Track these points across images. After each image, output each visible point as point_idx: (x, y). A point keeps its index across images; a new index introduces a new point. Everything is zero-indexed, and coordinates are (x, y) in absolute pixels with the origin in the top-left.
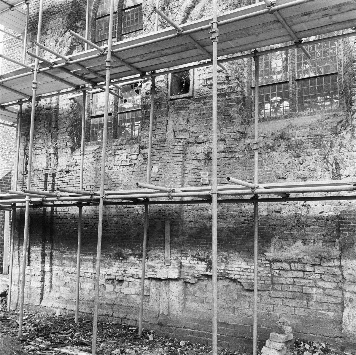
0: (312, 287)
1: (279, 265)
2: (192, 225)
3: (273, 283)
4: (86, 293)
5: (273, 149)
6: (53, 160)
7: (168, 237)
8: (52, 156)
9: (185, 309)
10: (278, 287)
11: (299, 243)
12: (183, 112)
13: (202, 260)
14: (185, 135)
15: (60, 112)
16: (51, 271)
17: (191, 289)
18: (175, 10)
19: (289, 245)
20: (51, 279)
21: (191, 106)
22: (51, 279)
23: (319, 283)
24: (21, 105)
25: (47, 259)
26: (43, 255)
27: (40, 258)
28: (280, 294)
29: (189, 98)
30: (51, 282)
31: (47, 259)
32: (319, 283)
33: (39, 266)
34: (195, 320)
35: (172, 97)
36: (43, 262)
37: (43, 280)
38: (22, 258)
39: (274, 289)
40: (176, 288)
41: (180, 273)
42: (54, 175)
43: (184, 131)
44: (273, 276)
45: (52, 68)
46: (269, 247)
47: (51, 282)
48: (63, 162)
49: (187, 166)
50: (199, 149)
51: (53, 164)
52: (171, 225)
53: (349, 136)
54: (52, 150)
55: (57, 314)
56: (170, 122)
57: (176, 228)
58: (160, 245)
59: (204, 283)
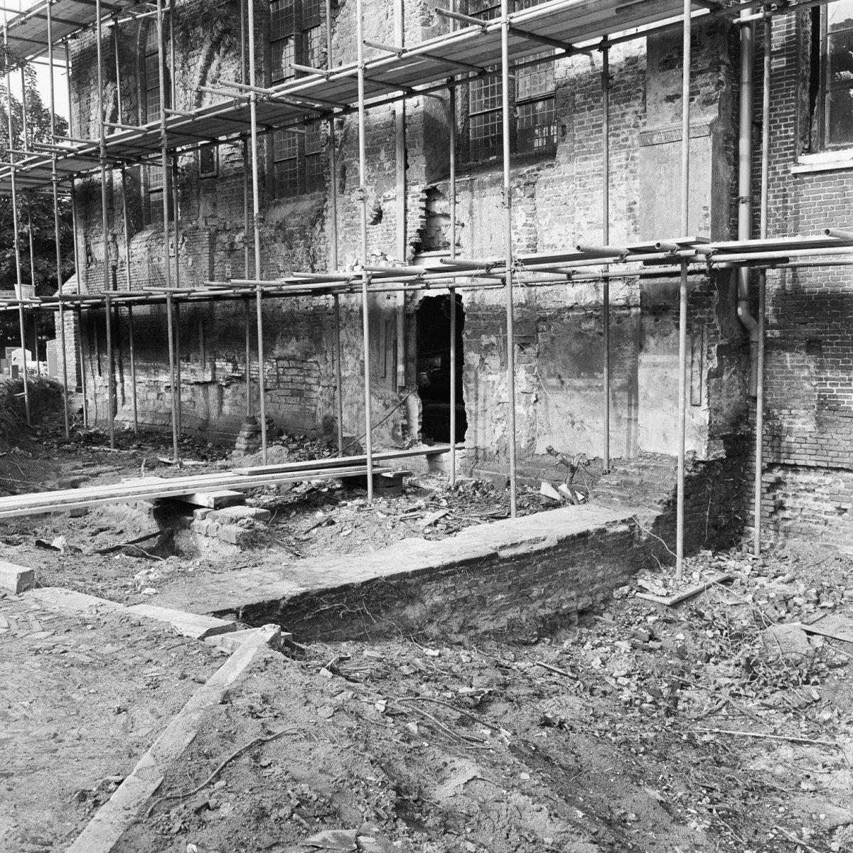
0: (302, 384)
1: (281, 363)
2: (221, 324)
3: (278, 382)
4: (152, 403)
5: (275, 241)
6: (112, 251)
7: (201, 339)
8: (111, 244)
9: (220, 412)
10: (282, 385)
11: (294, 340)
12: (209, 195)
13: (228, 361)
14: (215, 222)
15: (114, 188)
16: (122, 381)
17: (227, 392)
18: (192, 68)
19: (288, 342)
20: (123, 390)
21: (218, 188)
22: (123, 390)
23: (307, 380)
24: (73, 181)
25: (117, 369)
26: (113, 364)
27: (109, 367)
28: (283, 392)
29: (215, 177)
30: (123, 394)
31: (117, 369)
32: (307, 380)
33: (107, 375)
34: (226, 423)
35: (203, 176)
36: (113, 371)
37: (114, 391)
38: (96, 367)
39: (279, 388)
40: (213, 390)
41: (214, 376)
42: (114, 268)
43: (213, 217)
44: (278, 374)
45: (66, 158)
46: (274, 344)
47: (123, 394)
48: (123, 251)
49: (216, 258)
50: (224, 237)
51: (113, 255)
52: (204, 325)
53: (319, 228)
54: (110, 238)
55: (127, 428)
56: (202, 207)
57: (207, 327)
58: (197, 349)
59: (236, 385)
